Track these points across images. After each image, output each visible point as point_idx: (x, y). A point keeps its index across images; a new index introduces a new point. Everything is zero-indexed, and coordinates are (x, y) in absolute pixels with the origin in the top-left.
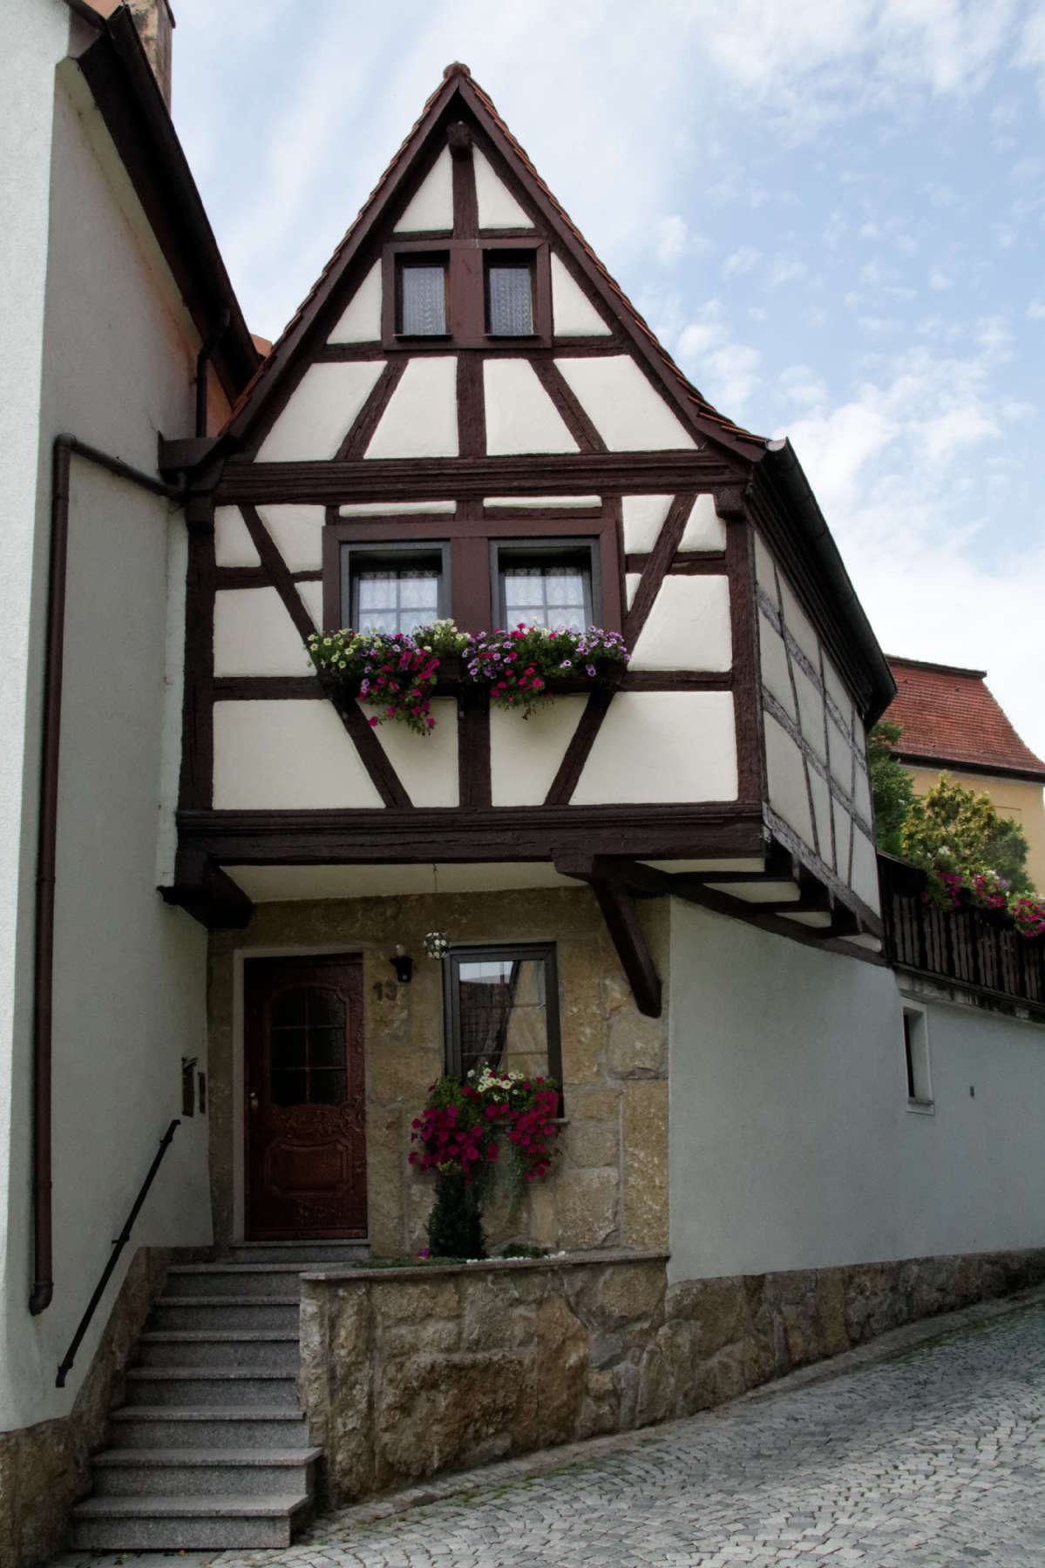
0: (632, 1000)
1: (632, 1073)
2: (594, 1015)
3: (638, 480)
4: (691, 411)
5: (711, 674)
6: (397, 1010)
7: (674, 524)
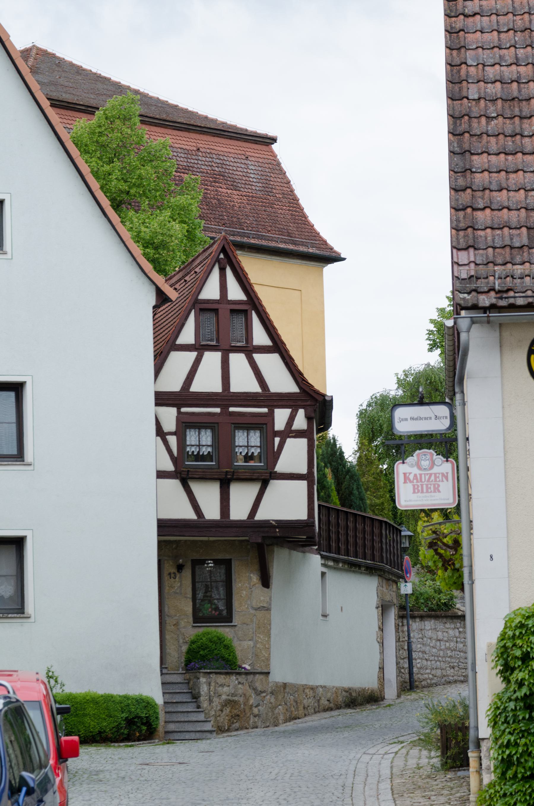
0: (260, 582)
1: (259, 608)
2: (247, 587)
3: (280, 403)
4: (300, 380)
5: (300, 474)
6: (176, 583)
7: (291, 419)
